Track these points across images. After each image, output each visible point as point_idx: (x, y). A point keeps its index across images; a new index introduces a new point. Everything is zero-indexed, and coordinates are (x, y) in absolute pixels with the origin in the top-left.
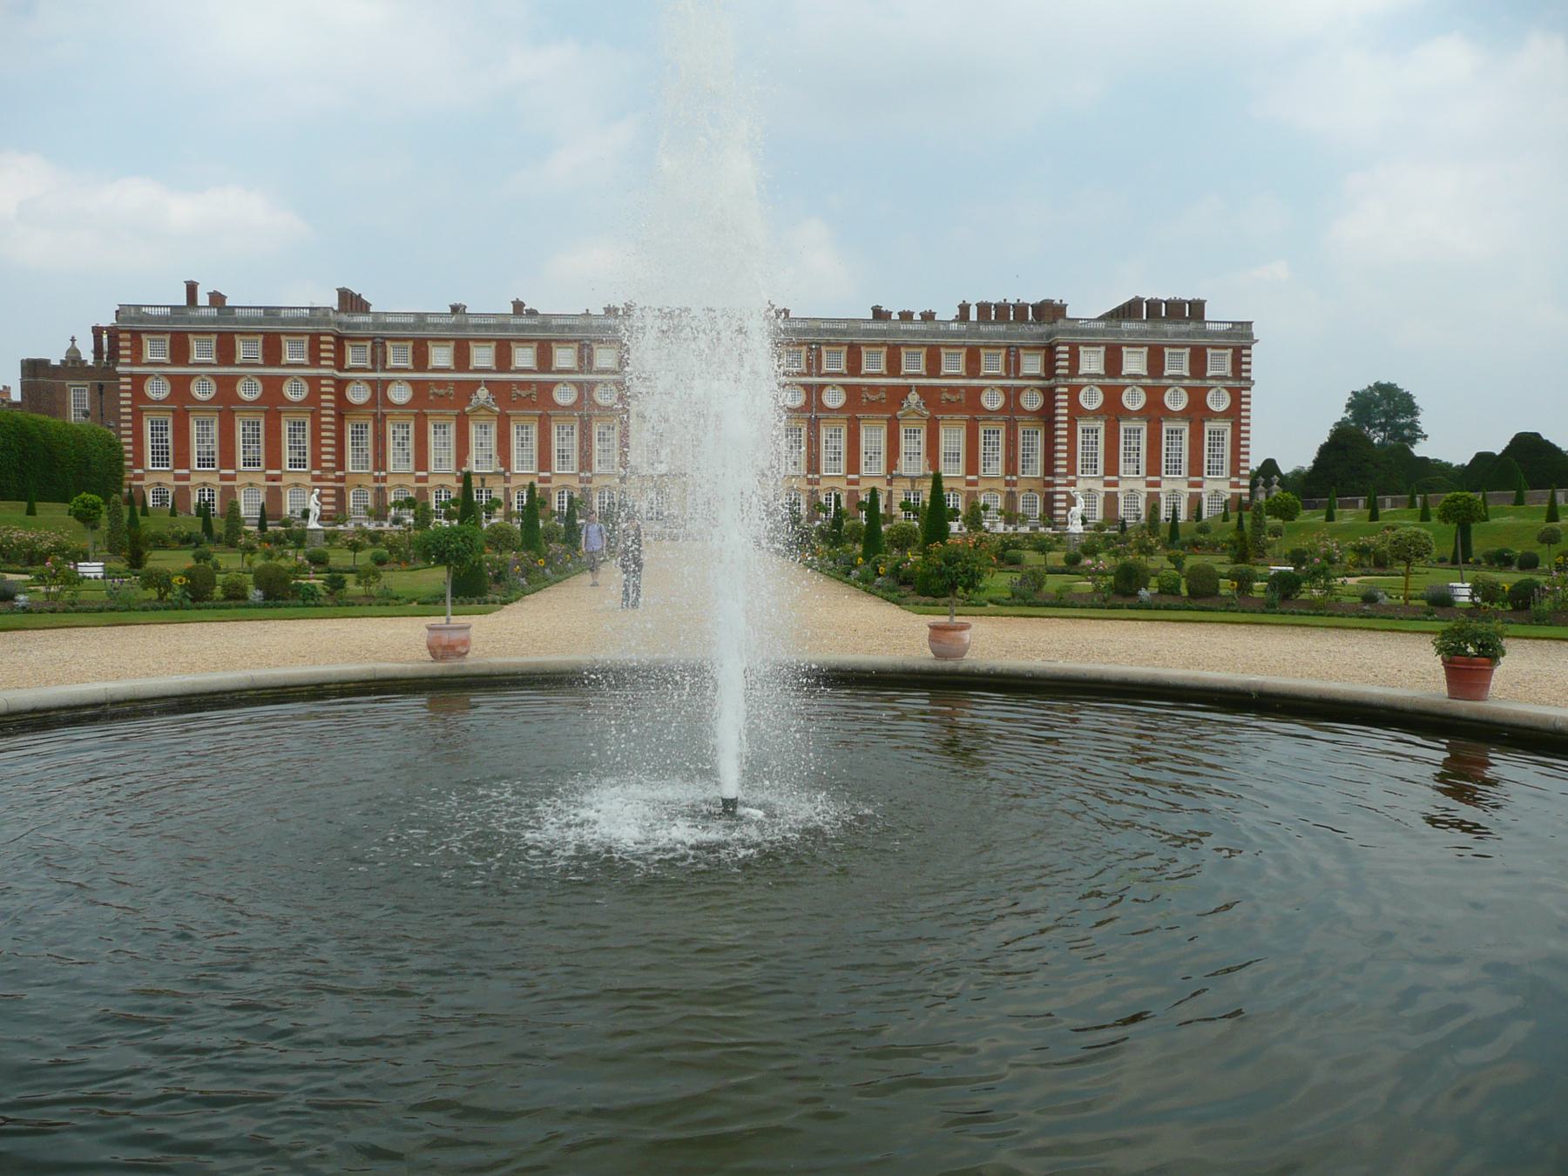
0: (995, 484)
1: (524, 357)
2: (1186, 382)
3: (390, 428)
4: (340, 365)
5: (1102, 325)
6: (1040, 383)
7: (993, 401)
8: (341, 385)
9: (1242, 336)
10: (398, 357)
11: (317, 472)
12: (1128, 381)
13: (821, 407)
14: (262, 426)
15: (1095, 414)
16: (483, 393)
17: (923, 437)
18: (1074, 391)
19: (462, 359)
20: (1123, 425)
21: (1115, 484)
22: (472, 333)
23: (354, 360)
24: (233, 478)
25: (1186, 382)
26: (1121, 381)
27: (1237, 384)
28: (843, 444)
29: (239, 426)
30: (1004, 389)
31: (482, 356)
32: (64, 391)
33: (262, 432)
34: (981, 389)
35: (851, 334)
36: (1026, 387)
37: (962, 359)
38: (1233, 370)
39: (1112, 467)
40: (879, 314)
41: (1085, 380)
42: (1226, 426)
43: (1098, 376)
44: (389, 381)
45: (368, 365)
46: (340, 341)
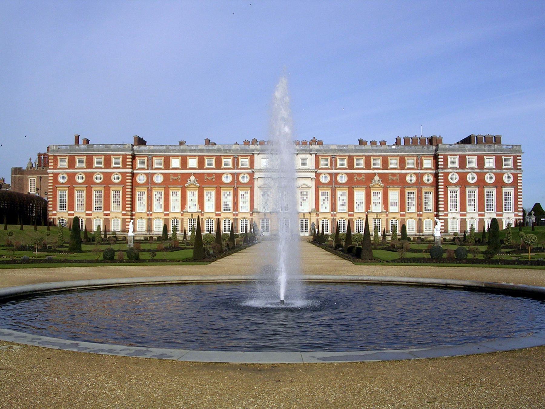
0: (412, 216)
1: (210, 163)
2: (494, 171)
3: (154, 193)
4: (133, 167)
5: (457, 146)
6: (432, 171)
7: (411, 179)
8: (133, 175)
9: (517, 151)
10: (158, 163)
11: (124, 212)
12: (469, 170)
13: (337, 183)
14: (103, 194)
15: (456, 185)
16: (192, 178)
17: (381, 195)
18: (446, 175)
19: (184, 164)
20: (468, 189)
21: (465, 215)
22: (188, 153)
23: (157, 165)
24: (90, 215)
25: (494, 171)
26: (466, 171)
27: (516, 172)
28: (346, 198)
29: (94, 193)
30: (416, 174)
31: (193, 163)
32: (27, 179)
33: (103, 196)
34: (406, 175)
35: (349, 151)
36: (426, 173)
37: (397, 161)
38: (514, 166)
40: (361, 142)
41: (451, 170)
42: (511, 190)
43: (456, 168)
44: (154, 174)
45: (146, 167)
46: (134, 157)
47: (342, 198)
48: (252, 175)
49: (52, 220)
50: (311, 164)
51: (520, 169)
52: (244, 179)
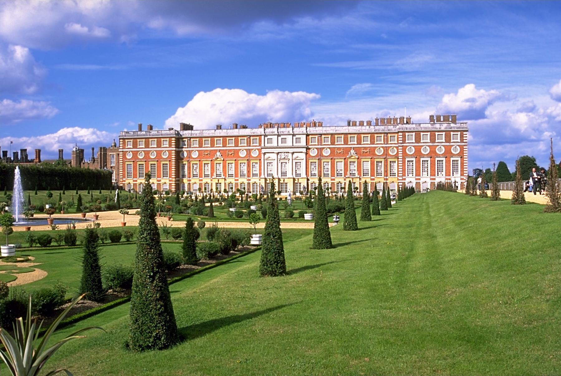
7: (379, 152)
15: (411, 156)
17: (356, 164)
18: (404, 148)
21: (419, 179)
39: (418, 174)
42: (459, 159)
47: (326, 167)
48: (260, 150)
49: (122, 185)
50: (303, 143)
51: (466, 142)
52: (255, 154)
